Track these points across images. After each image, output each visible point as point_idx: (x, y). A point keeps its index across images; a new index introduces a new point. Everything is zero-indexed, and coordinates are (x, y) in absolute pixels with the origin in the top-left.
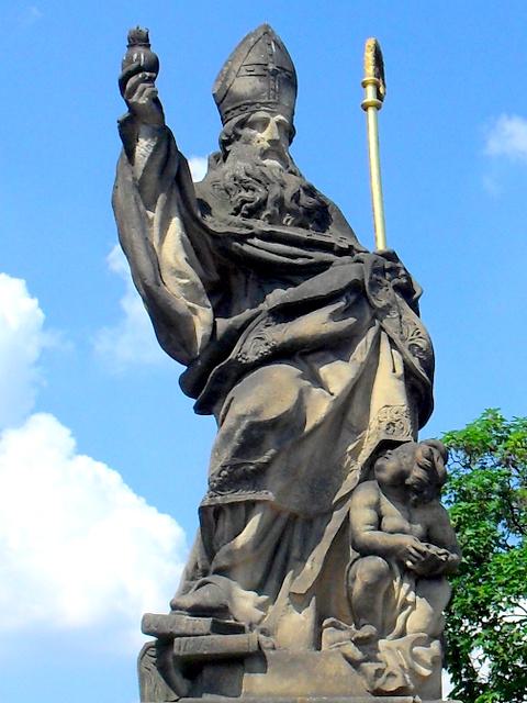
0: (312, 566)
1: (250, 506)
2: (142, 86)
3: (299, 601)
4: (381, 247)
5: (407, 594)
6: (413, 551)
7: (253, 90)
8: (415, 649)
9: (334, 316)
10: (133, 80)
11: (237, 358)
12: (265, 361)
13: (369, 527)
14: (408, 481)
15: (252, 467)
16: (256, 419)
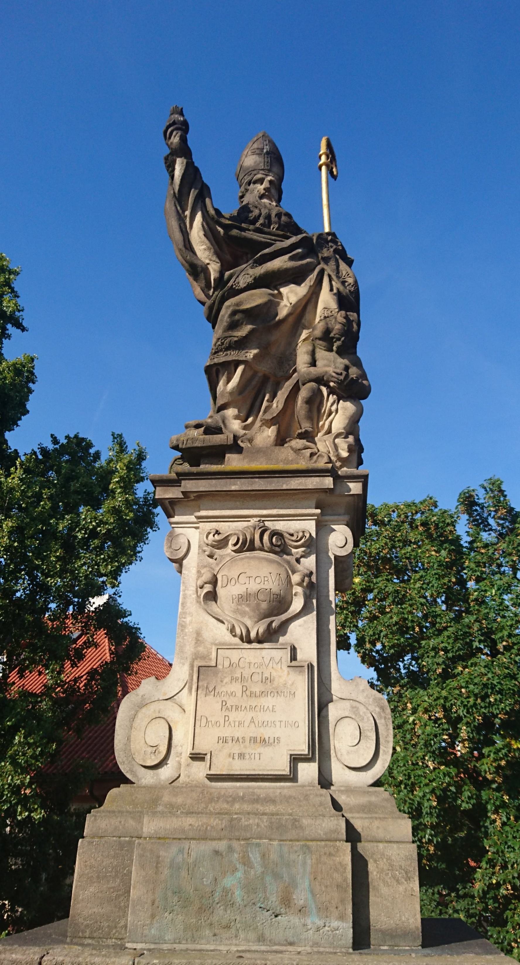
0: (278, 404)
1: (237, 364)
2: (174, 133)
3: (269, 423)
4: (327, 230)
5: (332, 405)
6: (334, 374)
7: (255, 162)
8: (337, 441)
9: (291, 259)
10: (170, 130)
11: (232, 285)
12: (249, 287)
13: (307, 365)
14: (332, 335)
15: (236, 339)
16: (237, 308)
